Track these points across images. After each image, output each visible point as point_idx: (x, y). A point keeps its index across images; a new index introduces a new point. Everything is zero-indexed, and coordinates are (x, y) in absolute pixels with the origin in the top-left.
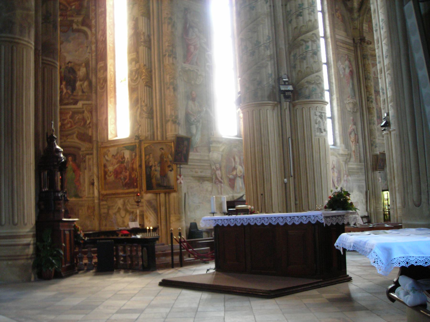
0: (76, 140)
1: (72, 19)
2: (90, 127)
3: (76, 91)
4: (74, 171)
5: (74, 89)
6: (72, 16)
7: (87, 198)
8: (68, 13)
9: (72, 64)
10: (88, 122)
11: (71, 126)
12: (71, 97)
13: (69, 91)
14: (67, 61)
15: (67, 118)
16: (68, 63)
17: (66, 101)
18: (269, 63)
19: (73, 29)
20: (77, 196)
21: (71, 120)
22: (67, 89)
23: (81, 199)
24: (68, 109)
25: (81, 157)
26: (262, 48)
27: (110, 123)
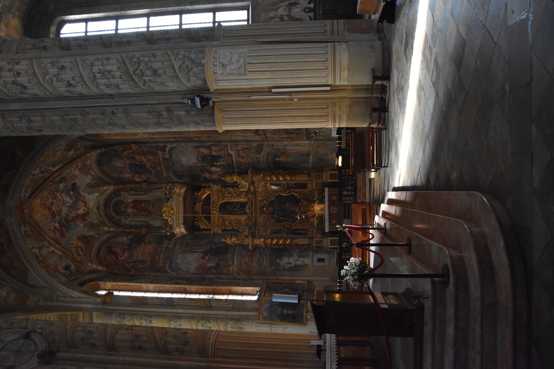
0: (262, 155)
1: (161, 158)
2: (250, 145)
3: (221, 155)
4: (288, 157)
5: (219, 157)
6: (159, 158)
7: (309, 147)
8: (157, 161)
9: (198, 158)
10: (246, 146)
11: (251, 158)
12: (226, 158)
13: (221, 160)
14: (197, 161)
15: (244, 161)
16: (199, 161)
18: (176, 113)
19: (169, 158)
20: (308, 155)
21: (245, 159)
22: (220, 161)
23: (311, 152)
24: (236, 161)
25: (275, 151)
26: (161, 120)
27: (245, 134)
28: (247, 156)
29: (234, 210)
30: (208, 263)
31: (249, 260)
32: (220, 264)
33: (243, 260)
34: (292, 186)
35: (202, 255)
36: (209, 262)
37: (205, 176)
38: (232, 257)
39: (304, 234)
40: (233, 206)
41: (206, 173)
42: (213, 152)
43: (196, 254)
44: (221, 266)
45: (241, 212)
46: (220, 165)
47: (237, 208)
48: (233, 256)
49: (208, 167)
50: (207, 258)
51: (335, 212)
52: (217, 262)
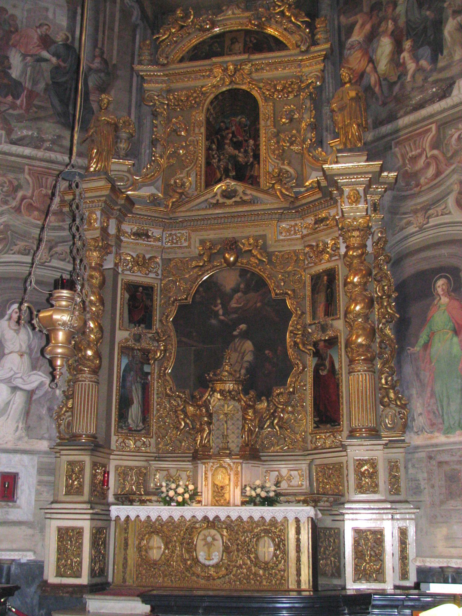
3: (445, 52)
11: (438, 174)
13: (423, 63)
15: (424, 150)
17: (418, 98)
21: (435, 152)
22: (416, 59)
28: (449, 155)
29: (228, 141)
30: (24, 56)
31: (24, 198)
32: (16, 96)
33: (28, 177)
34: (327, 363)
35: (59, 38)
36: (29, 58)
37: (357, 27)
38: (43, 141)
39: (122, 416)
40: (240, 139)
41: (368, 27)
42: (454, 19)
43: (63, 21)
44: (10, 99)
45: (219, 167)
46: (404, 64)
47: (236, 152)
48: (47, 144)
49: (391, 25)
50: (45, 54)
51: (202, 556)
52: (28, 85)
